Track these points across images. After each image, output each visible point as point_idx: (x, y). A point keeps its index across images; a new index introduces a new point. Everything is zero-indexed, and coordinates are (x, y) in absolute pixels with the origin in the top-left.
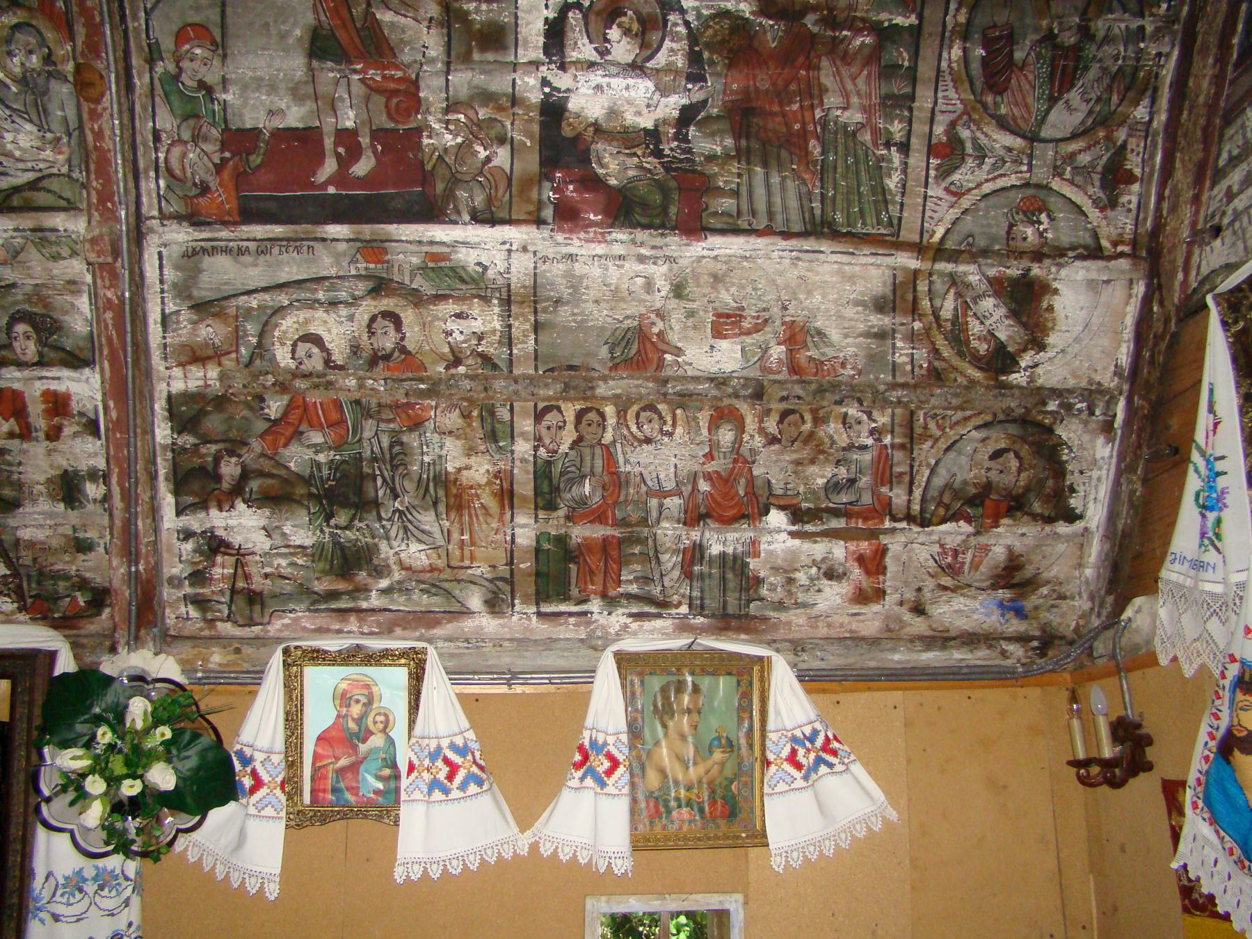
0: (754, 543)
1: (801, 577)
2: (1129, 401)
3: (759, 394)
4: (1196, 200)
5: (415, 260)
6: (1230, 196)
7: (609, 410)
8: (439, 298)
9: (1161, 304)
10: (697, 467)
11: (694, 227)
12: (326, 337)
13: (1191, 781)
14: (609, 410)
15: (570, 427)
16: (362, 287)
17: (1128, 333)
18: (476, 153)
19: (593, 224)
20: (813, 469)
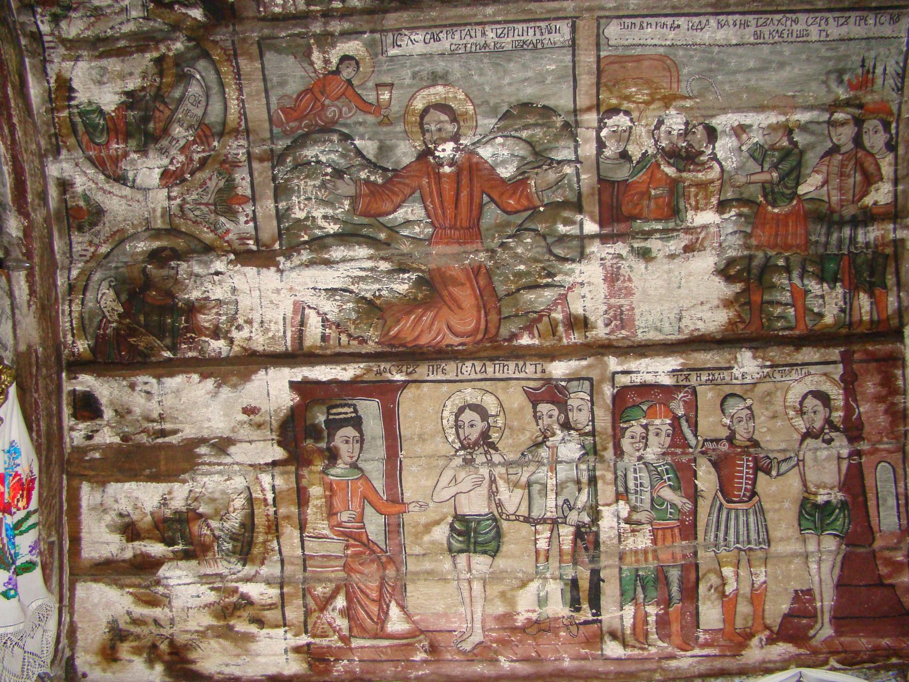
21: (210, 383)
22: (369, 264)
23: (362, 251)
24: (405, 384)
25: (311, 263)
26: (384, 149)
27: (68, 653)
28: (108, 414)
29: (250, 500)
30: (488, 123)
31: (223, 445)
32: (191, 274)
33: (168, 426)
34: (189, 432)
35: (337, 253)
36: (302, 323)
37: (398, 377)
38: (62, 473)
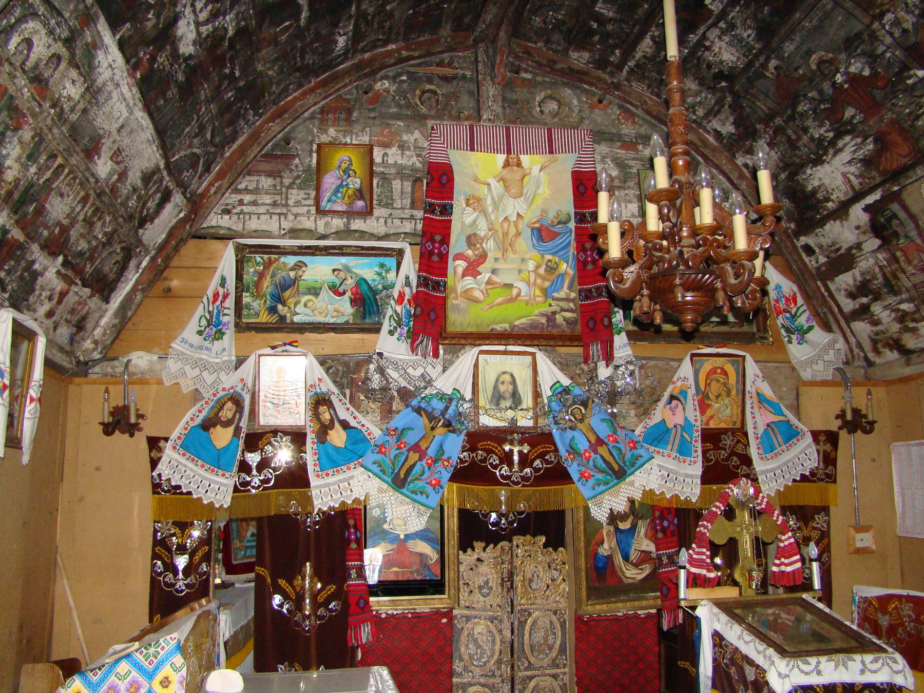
0: (46, 269)
1: (44, 294)
2: (153, 259)
3: (99, 195)
4: (223, 195)
5: (89, 40)
6: (241, 202)
7: (67, 171)
8: (78, 67)
9: (191, 227)
10: (61, 219)
11: (148, 107)
12: (35, 49)
13: (173, 436)
14: (67, 171)
15: (51, 170)
16: (65, 34)
17: (167, 231)
18: (149, 13)
19: (135, 78)
20: (82, 241)
21: (838, 222)
22: (853, 143)
23: (848, 138)
24: (900, 190)
25: (835, 154)
26: (821, 92)
27: (862, 354)
28: (817, 250)
29: (880, 267)
30: (843, 56)
31: (859, 246)
32: (804, 180)
33: (837, 246)
34: (845, 246)
35: (840, 144)
36: (850, 181)
37: (896, 188)
38: (816, 281)
